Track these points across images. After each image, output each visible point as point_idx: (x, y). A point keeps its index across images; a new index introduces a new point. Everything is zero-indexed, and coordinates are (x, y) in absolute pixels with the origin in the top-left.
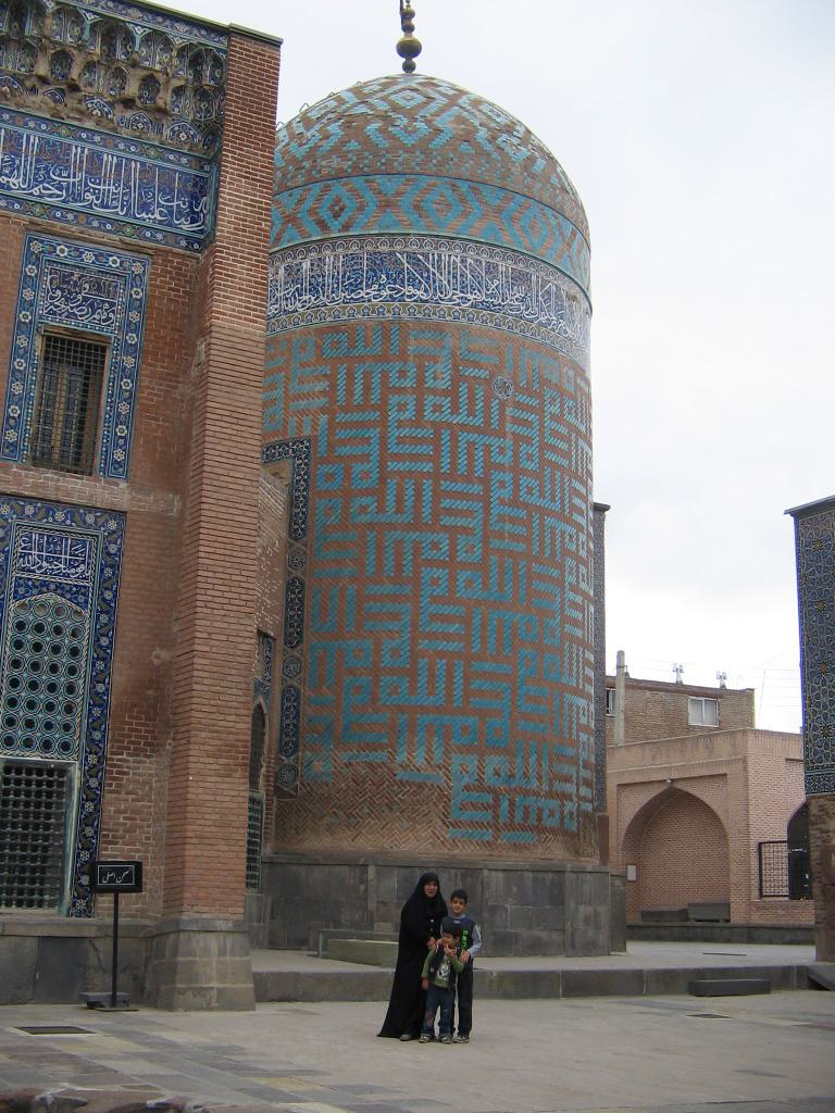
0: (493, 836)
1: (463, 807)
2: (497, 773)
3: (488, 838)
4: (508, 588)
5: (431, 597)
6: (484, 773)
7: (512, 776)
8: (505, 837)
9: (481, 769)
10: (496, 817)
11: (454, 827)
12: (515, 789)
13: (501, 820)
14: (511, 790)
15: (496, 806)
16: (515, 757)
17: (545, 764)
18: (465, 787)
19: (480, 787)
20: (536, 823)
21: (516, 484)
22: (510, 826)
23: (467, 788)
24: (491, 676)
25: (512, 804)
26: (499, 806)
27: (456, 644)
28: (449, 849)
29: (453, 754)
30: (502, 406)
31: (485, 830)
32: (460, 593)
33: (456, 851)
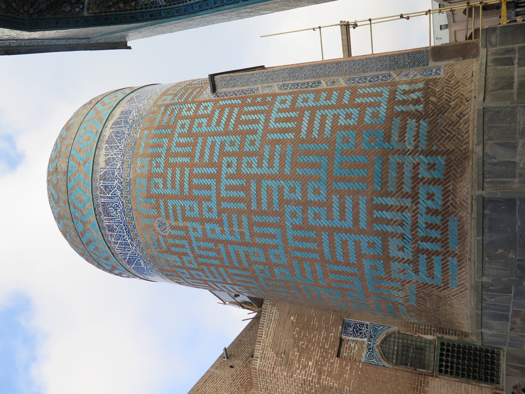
0: (453, 257)
1: (431, 275)
2: (402, 249)
3: (455, 261)
4: (272, 231)
5: (293, 277)
6: (403, 259)
7: (402, 236)
8: (454, 246)
9: (401, 260)
10: (437, 253)
11: (448, 284)
12: (412, 235)
13: (440, 250)
14: (414, 239)
15: (430, 254)
16: (387, 232)
17: (390, 201)
18: (415, 273)
19: (415, 262)
20: (440, 217)
21: (210, 221)
22: (445, 242)
23: (416, 271)
24: (332, 247)
25: (425, 239)
26: (428, 250)
27: (316, 267)
28: (466, 289)
29: (392, 276)
30: (173, 228)
31: (449, 263)
32: (285, 263)
33: (468, 285)
